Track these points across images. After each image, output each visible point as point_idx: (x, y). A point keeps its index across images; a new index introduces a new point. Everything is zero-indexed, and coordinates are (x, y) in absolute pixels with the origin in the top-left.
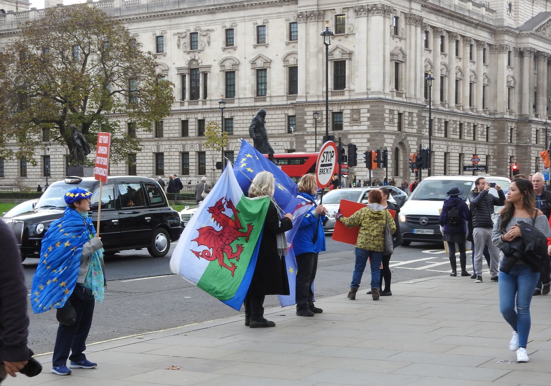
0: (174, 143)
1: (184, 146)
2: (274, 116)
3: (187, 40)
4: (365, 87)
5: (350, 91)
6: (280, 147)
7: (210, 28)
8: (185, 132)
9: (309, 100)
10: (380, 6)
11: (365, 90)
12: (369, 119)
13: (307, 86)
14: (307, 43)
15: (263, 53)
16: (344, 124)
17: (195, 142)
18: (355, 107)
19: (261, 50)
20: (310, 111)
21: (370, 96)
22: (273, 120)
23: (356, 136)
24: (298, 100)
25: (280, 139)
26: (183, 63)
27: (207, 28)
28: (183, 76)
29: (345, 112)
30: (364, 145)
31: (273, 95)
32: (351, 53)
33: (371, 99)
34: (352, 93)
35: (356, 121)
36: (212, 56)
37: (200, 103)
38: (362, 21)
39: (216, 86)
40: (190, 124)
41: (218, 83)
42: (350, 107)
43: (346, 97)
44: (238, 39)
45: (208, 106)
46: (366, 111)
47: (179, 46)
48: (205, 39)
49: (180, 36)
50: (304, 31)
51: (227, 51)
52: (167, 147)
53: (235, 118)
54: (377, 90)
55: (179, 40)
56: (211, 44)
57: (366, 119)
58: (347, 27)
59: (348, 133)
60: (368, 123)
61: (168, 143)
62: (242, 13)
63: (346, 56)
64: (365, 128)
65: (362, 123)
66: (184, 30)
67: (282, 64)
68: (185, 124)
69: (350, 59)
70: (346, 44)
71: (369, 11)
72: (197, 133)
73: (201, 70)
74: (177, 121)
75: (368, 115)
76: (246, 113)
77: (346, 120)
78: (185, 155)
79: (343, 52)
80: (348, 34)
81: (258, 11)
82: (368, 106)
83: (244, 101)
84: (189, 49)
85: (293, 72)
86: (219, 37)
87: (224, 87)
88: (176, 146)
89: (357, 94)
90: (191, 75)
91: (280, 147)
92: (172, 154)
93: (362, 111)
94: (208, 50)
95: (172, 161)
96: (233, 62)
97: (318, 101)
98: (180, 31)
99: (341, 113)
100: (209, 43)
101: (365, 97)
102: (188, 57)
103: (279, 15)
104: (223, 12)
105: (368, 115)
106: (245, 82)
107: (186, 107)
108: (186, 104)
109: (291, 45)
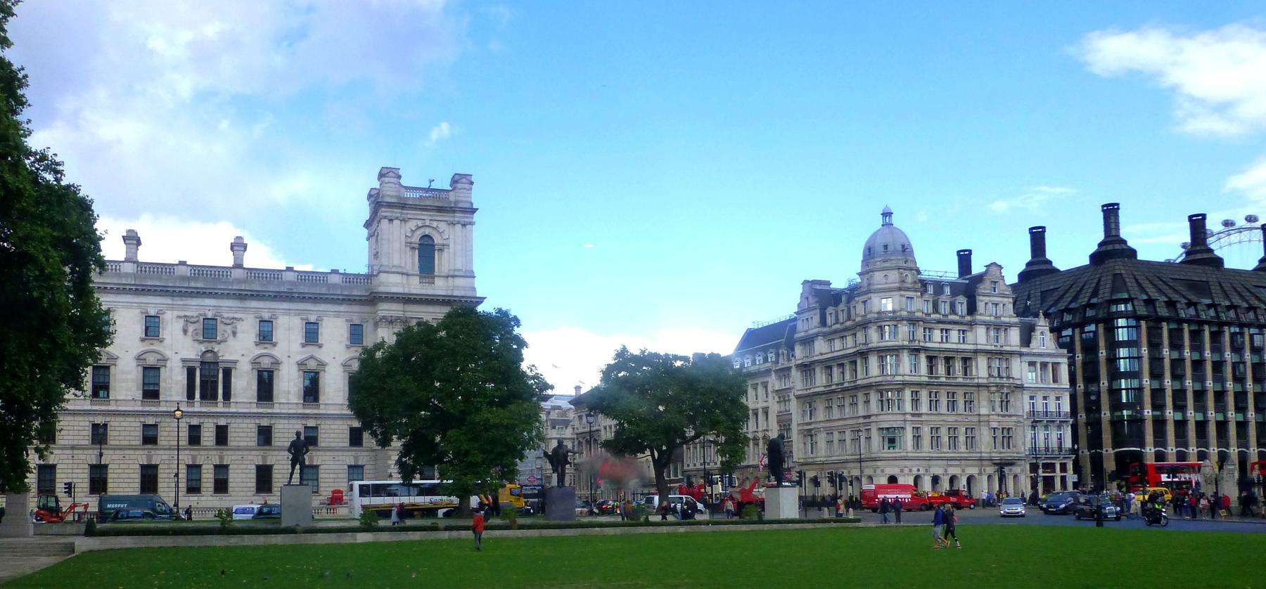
19: (311, 350)
27: (231, 315)
28: (191, 373)
37: (220, 405)
39: (244, 385)
47: (185, 332)
48: (229, 329)
52: (165, 457)
53: (277, 426)
62: (285, 305)
66: (195, 314)
78: (194, 469)
94: (231, 341)
100: (234, 333)
103: (338, 314)
107: (197, 407)
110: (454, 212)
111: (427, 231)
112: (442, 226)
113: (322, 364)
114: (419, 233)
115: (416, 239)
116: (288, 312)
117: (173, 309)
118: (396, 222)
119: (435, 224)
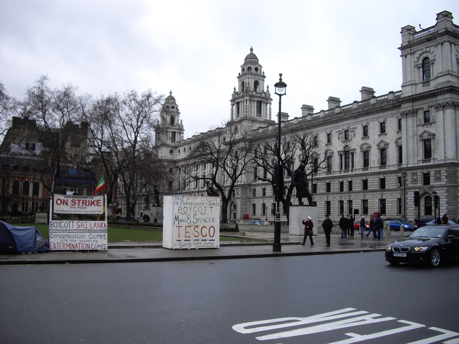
0: (335, 195)
1: (341, 197)
2: (390, 178)
3: (343, 135)
4: (443, 156)
5: (434, 159)
6: (394, 197)
7: (355, 126)
8: (342, 189)
9: (409, 166)
10: (451, 102)
11: (444, 158)
12: (446, 177)
13: (408, 157)
14: (407, 130)
15: (384, 139)
16: (431, 181)
17: (347, 195)
18: (437, 169)
19: (383, 138)
20: (409, 173)
21: (447, 162)
22: (390, 180)
23: (439, 189)
24: (403, 166)
25: (394, 192)
26: (341, 149)
29: (431, 173)
30: (443, 194)
31: (390, 164)
32: (434, 135)
33: (447, 163)
34: (436, 161)
35: (438, 179)
36: (356, 142)
37: (350, 171)
38: (441, 113)
40: (344, 184)
41: (360, 159)
42: (434, 170)
43: (432, 163)
44: (370, 132)
45: (354, 173)
46: (444, 171)
48: (352, 134)
49: (340, 133)
50: (405, 123)
51: (364, 139)
52: (332, 198)
54: (451, 157)
55: (339, 135)
56: (356, 136)
57: (444, 177)
58: (431, 118)
59: (433, 187)
60: (446, 180)
61: (333, 195)
62: (372, 116)
63: (431, 137)
64: (444, 183)
65: (442, 180)
66: (341, 129)
67: (394, 145)
68: (342, 184)
69: (434, 139)
70: (431, 129)
71: (444, 107)
72: (348, 190)
73: (350, 152)
74: (338, 182)
75: (446, 174)
76: (375, 176)
77: (432, 178)
78: (341, 202)
79: (430, 134)
80: (432, 123)
81: (381, 114)
82: (445, 169)
83: (373, 169)
84: (344, 140)
85: (400, 148)
86: (359, 132)
87: (363, 161)
88: (337, 197)
89: (439, 161)
90: (345, 155)
91: (394, 197)
92: (335, 202)
93: (442, 172)
94: (354, 140)
95: (335, 206)
96: (367, 146)
97: (414, 167)
98: (340, 130)
99: (428, 174)
100: (354, 135)
101: (444, 162)
102: (344, 145)
104: (362, 117)
105: (446, 174)
106: (374, 157)
107: (343, 174)
108: (343, 172)
109: (400, 133)
110: (436, 38)
111: (425, 55)
112: (432, 49)
113: (387, 144)
114: (422, 58)
115: (420, 62)
116: (373, 120)
117: (335, 129)
118: (409, 56)
119: (428, 50)
